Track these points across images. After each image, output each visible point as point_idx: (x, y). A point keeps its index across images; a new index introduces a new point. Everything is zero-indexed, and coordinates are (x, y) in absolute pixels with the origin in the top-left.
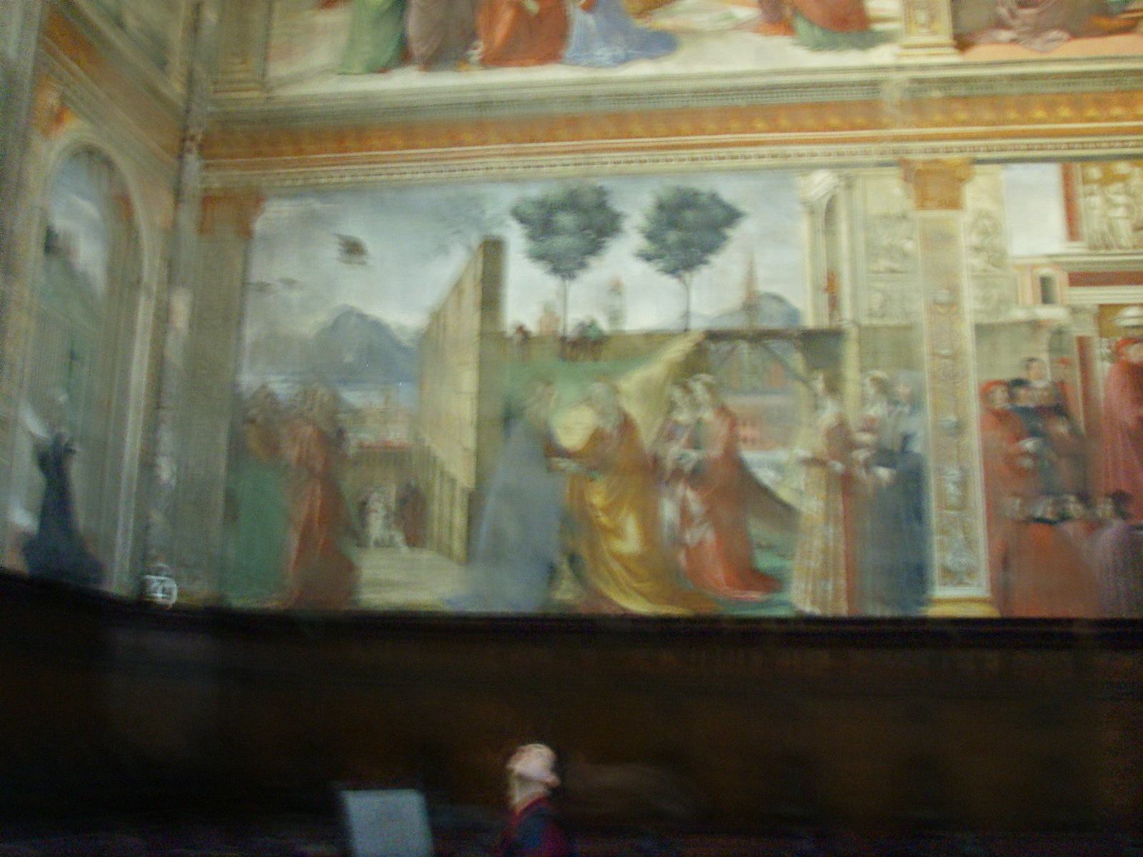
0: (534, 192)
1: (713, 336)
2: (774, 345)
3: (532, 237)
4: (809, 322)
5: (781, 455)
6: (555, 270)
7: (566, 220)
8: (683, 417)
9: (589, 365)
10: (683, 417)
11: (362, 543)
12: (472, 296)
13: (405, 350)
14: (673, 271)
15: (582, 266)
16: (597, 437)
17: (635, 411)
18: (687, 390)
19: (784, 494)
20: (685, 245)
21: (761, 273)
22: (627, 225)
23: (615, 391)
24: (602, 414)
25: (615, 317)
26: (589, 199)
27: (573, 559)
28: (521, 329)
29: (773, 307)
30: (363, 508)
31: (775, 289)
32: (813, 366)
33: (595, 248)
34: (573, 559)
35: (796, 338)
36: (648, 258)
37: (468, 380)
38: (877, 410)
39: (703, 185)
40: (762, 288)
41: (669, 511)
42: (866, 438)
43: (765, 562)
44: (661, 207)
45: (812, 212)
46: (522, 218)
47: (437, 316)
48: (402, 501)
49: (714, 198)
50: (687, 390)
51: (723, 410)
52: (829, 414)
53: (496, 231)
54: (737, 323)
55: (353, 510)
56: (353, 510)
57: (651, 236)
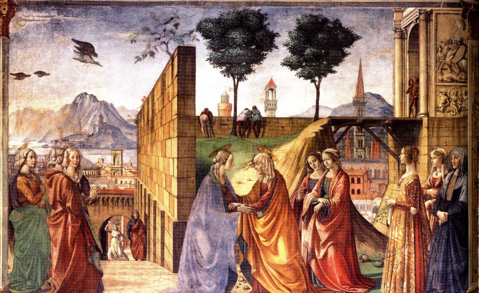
0: (215, 14)
1: (335, 121)
2: (376, 130)
3: (211, 47)
4: (397, 115)
5: (377, 202)
6: (228, 72)
7: (237, 35)
8: (316, 175)
9: (253, 140)
10: (316, 175)
11: (104, 257)
12: (173, 89)
13: (125, 124)
14: (309, 76)
15: (250, 71)
16: (259, 187)
17: (285, 171)
18: (319, 158)
19: (380, 227)
20: (317, 58)
21: (367, 79)
22: (278, 41)
23: (271, 157)
24: (263, 174)
25: (271, 105)
26: (253, 20)
27: (245, 267)
28: (207, 112)
29: (374, 102)
30: (104, 235)
31: (374, 92)
32: (399, 146)
33: (258, 58)
34: (245, 267)
35: (388, 125)
36: (292, 66)
37: (172, 146)
38: (439, 174)
39: (330, 14)
40: (367, 90)
41: (306, 236)
42: (432, 192)
43: (366, 270)
44: (301, 28)
45: (402, 38)
46: (206, 36)
47: (149, 100)
48: (130, 230)
49: (337, 22)
50: (319, 158)
51: (340, 172)
52: (408, 175)
53: (188, 43)
54: (351, 113)
55: (96, 234)
56: (96, 234)
57: (293, 50)
